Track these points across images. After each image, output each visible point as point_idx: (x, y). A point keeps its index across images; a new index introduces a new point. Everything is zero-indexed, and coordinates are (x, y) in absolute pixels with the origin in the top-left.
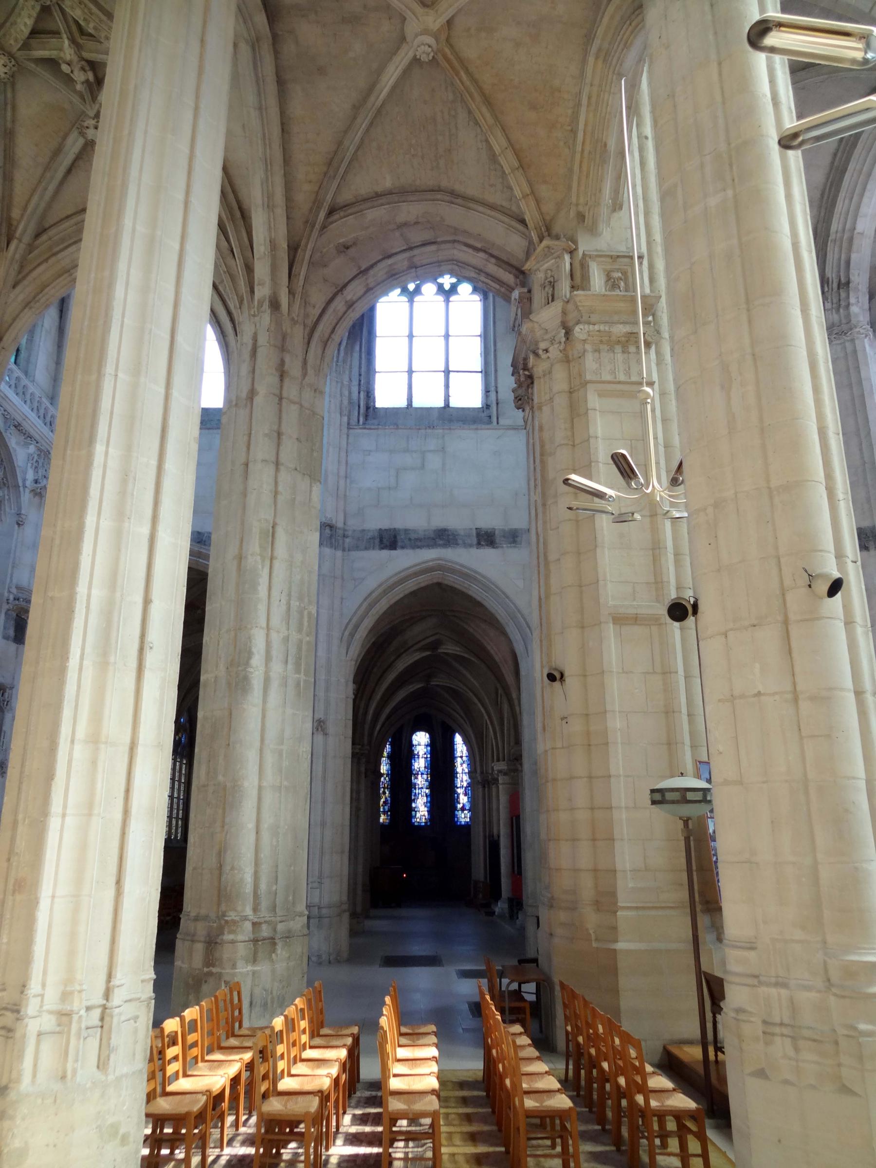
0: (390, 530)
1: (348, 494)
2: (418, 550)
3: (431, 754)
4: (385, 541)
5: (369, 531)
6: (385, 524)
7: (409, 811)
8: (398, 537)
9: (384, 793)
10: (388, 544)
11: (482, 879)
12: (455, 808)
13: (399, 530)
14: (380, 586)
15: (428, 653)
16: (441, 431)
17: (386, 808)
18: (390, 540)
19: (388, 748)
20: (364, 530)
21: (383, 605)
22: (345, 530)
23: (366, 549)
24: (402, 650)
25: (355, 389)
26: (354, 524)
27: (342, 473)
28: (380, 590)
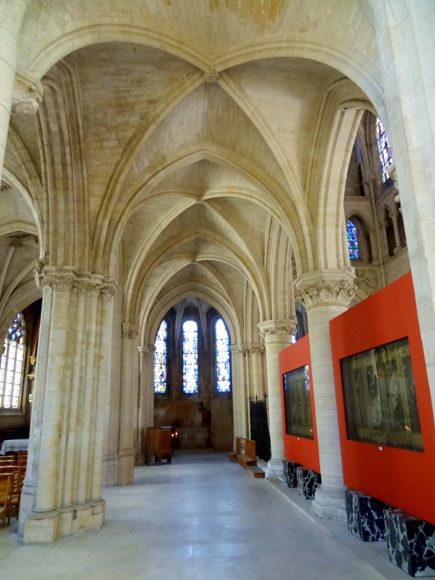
3: (199, 337)
7: (181, 381)
9: (161, 368)
11: (245, 436)
12: (217, 379)
15: (193, 202)
17: (163, 380)
19: (162, 333)
24: (160, 168)
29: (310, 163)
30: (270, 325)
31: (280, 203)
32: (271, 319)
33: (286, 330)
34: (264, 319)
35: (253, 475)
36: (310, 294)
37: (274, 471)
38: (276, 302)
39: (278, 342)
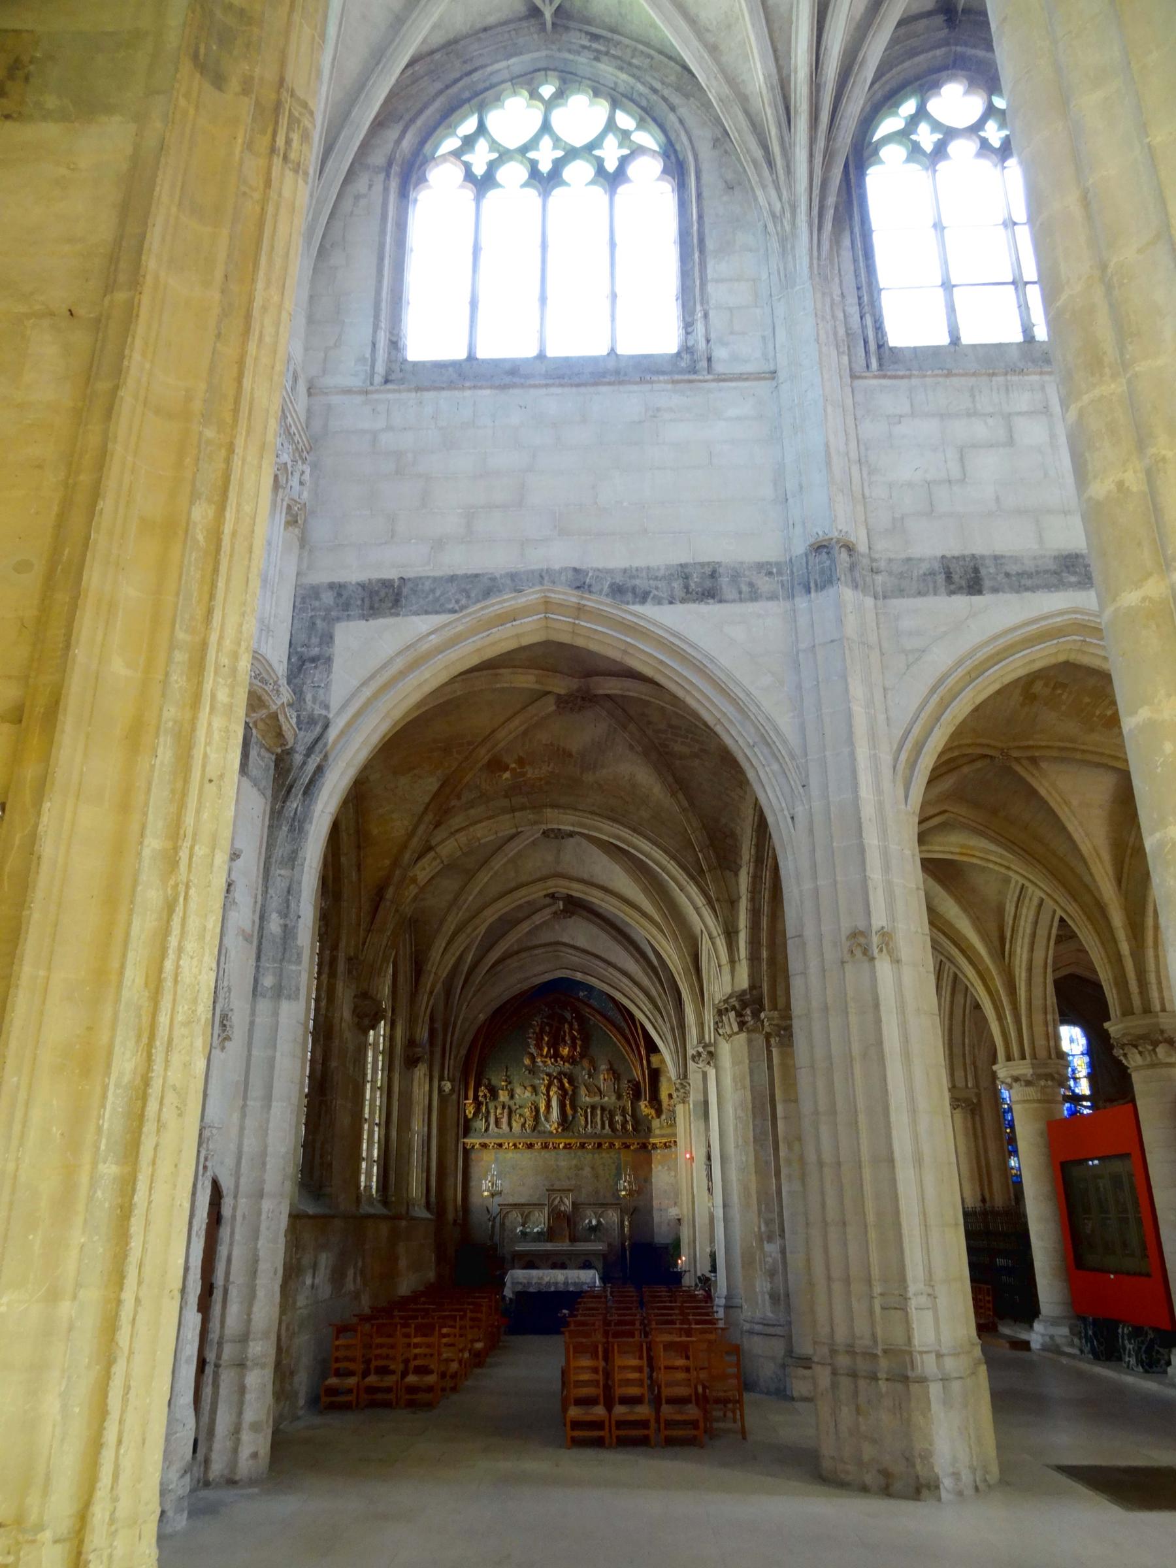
0: (963, 558)
1: (867, 493)
2: (1028, 595)
4: (956, 577)
5: (921, 560)
6: (953, 548)
8: (983, 572)
10: (963, 583)
13: (983, 557)
14: (960, 663)
16: (1036, 378)
18: (967, 577)
20: (909, 560)
21: (961, 709)
22: (873, 560)
23: (920, 594)
25: (854, 310)
26: (886, 548)
27: (854, 455)
28: (960, 672)
29: (1129, 851)
30: (1024, 1069)
31: (1075, 900)
32: (1023, 1058)
33: (1053, 1079)
34: (1009, 1058)
35: (1007, 1345)
36: (1140, 1049)
37: (1052, 1337)
38: (1031, 1026)
39: (1039, 1101)
